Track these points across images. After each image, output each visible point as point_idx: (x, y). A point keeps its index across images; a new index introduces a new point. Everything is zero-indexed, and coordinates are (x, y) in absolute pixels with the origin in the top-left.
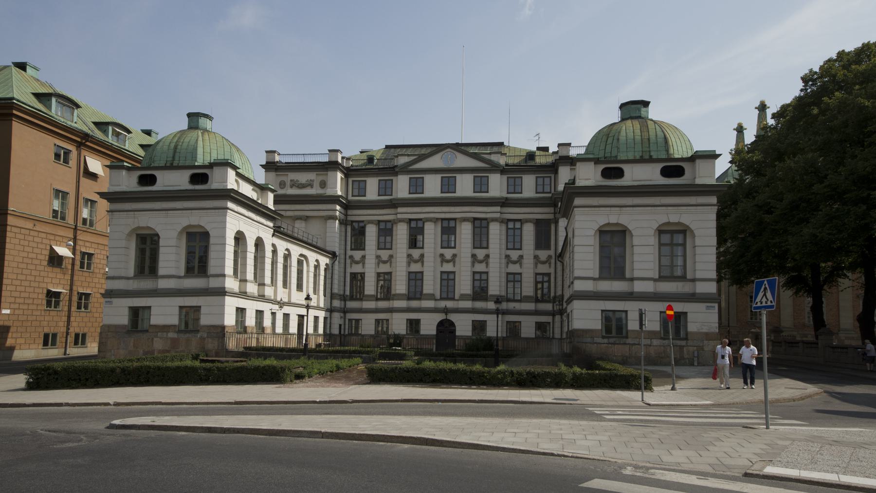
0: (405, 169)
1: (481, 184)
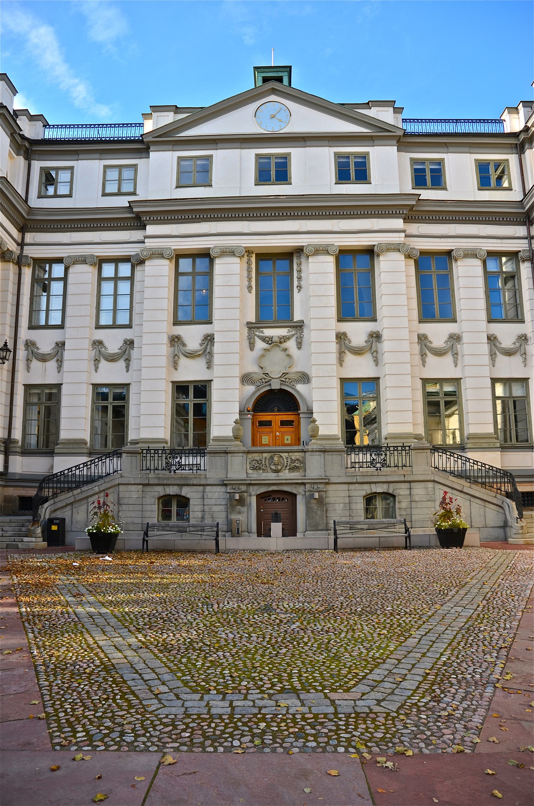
0: (166, 138)
1: (354, 170)
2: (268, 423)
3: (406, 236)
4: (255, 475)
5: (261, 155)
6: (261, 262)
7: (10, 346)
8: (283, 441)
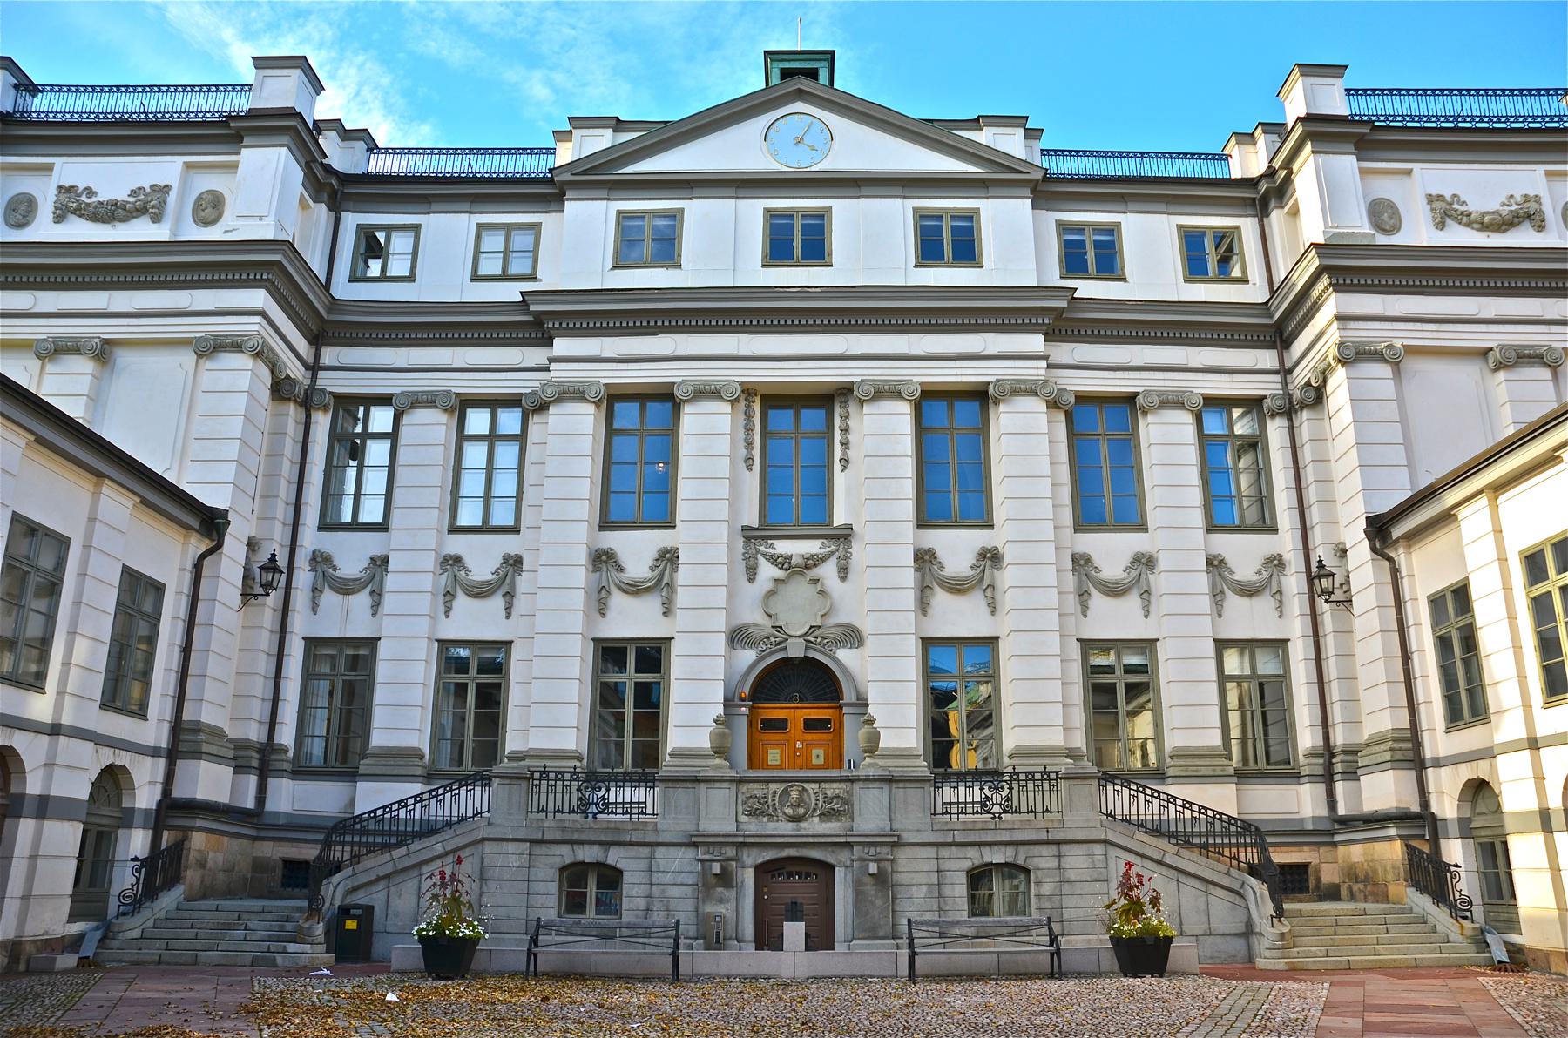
0: (595, 177)
1: (949, 241)
2: (781, 724)
3: (1049, 367)
4: (752, 827)
5: (775, 210)
6: (771, 413)
7: (282, 562)
8: (808, 757)
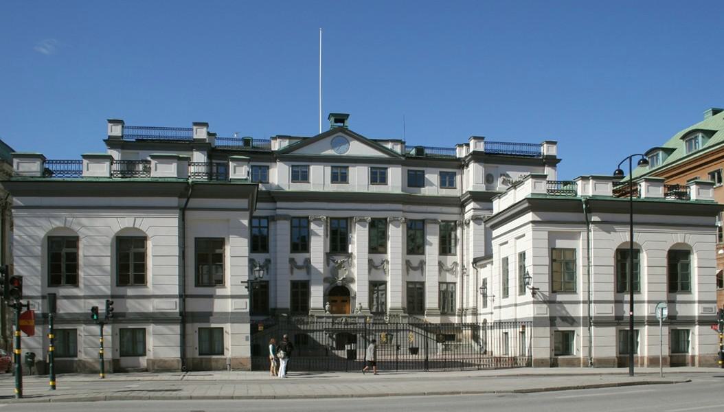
2: (336, 301)
